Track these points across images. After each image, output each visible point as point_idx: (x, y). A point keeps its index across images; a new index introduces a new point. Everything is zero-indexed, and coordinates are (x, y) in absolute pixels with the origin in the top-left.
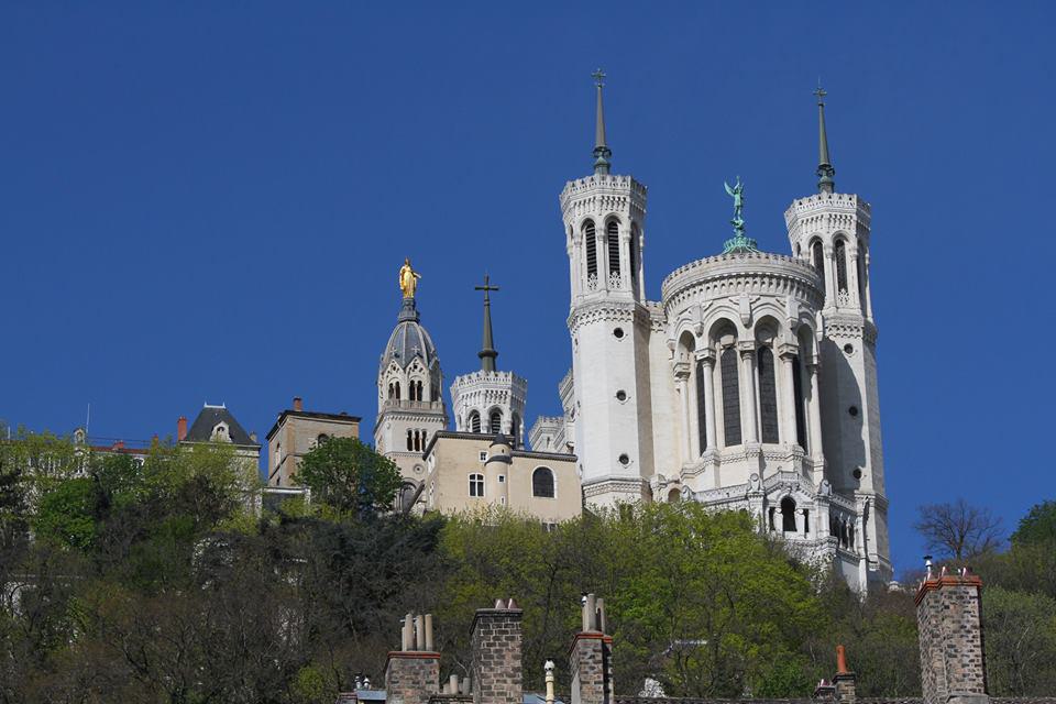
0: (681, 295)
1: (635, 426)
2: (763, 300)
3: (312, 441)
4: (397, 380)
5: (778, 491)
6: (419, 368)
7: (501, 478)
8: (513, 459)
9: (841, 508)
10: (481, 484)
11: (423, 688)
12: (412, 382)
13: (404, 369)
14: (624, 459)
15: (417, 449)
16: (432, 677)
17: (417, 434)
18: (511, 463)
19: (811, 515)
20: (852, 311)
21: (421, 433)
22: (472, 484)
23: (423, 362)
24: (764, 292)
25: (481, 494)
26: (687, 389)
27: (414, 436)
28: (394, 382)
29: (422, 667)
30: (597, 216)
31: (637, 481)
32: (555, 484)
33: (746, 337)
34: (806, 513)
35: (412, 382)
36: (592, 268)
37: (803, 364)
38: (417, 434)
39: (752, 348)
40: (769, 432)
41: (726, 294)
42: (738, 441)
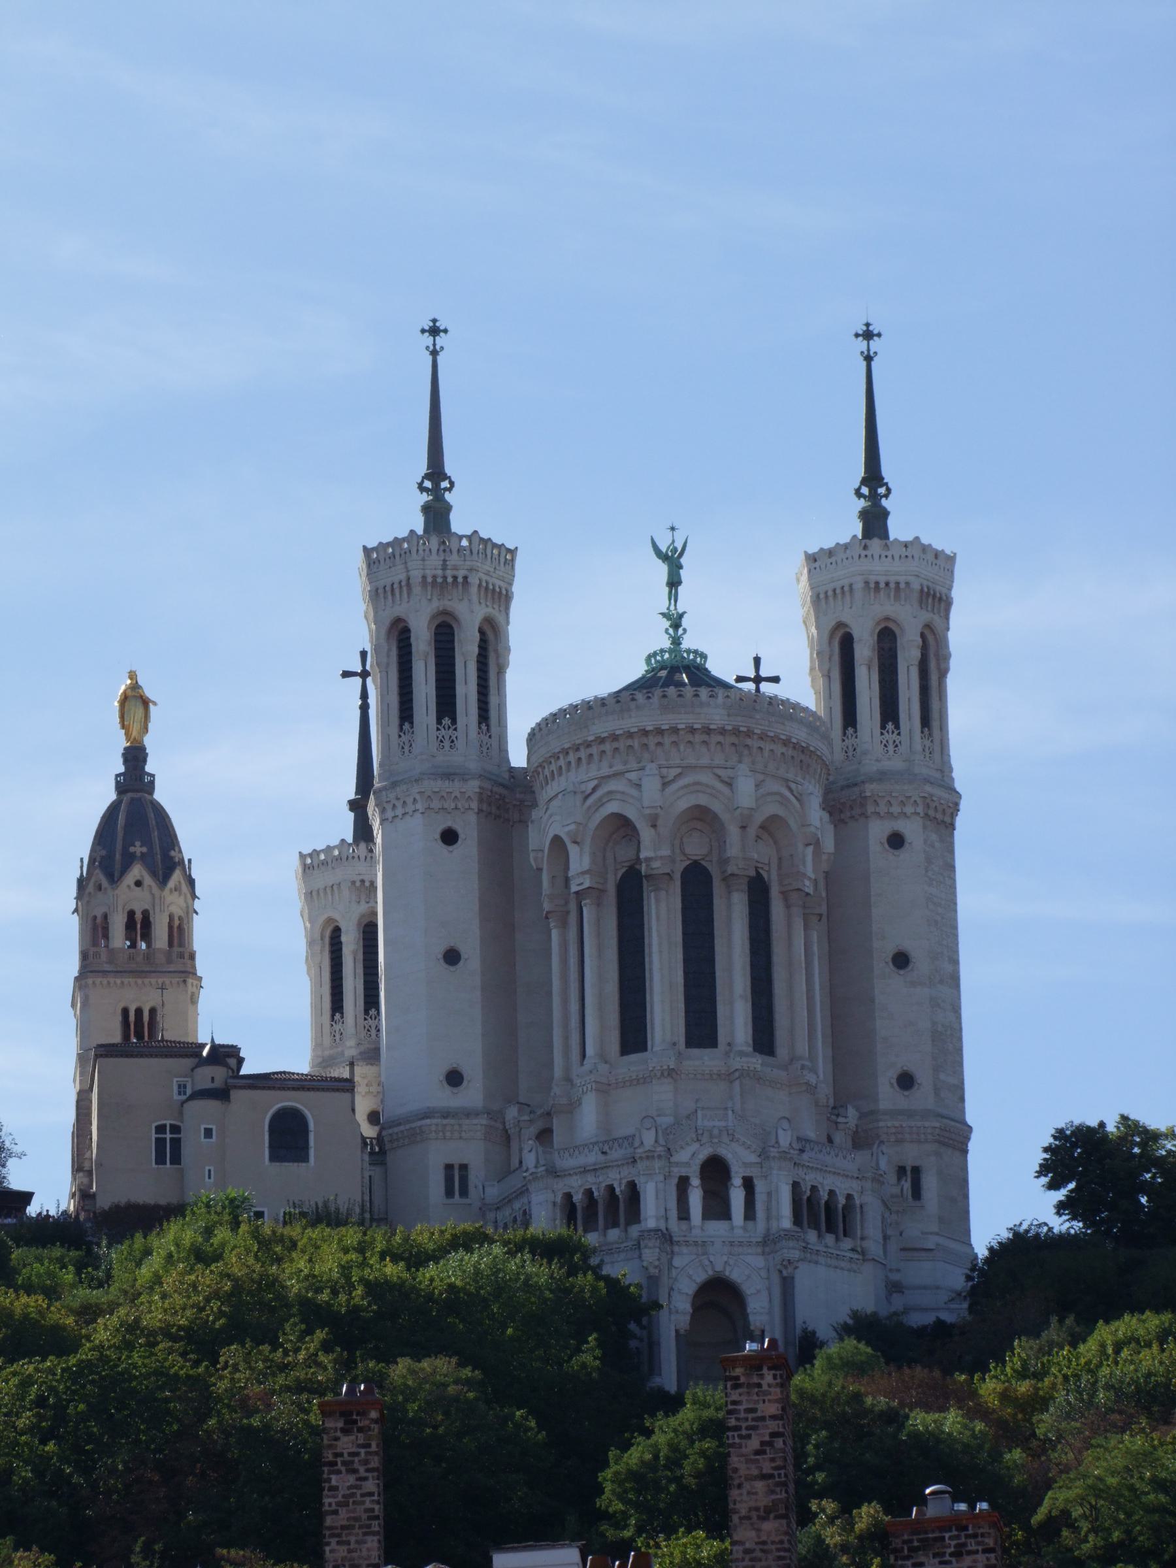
7: (208, 1133)
10: (176, 1143)
12: (131, 914)
14: (454, 1078)
17: (139, 1012)
19: (760, 1187)
22: (160, 1143)
24: (691, 761)
25: (176, 1159)
34: (748, 1184)
38: (139, 1012)
41: (619, 767)
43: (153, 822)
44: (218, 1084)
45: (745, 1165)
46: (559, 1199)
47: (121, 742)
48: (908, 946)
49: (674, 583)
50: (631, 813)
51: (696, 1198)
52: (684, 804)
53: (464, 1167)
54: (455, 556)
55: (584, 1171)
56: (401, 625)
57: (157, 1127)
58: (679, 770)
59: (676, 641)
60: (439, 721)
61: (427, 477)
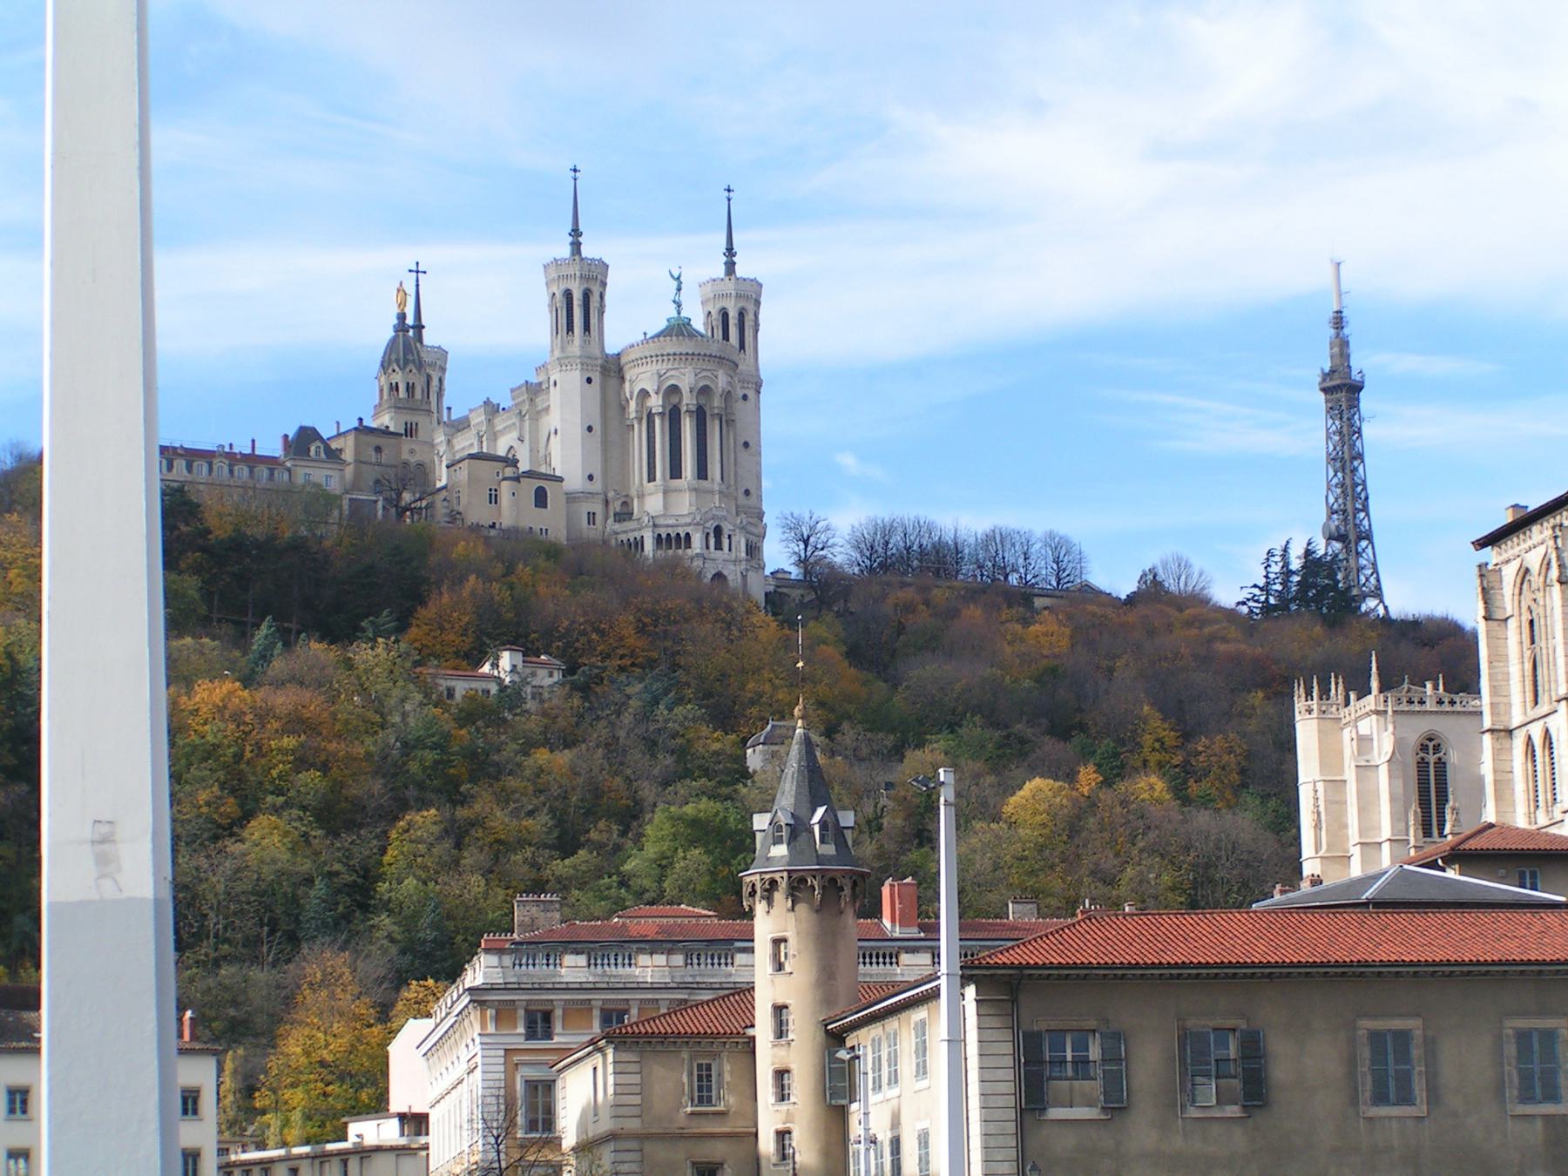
0: (639, 362)
1: (599, 452)
2: (704, 374)
10: (496, 495)
14: (591, 478)
18: (519, 482)
19: (733, 539)
22: (491, 495)
27: (409, 425)
32: (549, 499)
33: (688, 401)
34: (729, 537)
37: (724, 420)
40: (702, 472)
41: (676, 366)
45: (730, 530)
46: (656, 535)
47: (395, 310)
48: (748, 440)
49: (679, 289)
51: (712, 541)
52: (701, 384)
53: (594, 514)
55: (668, 526)
59: (679, 313)
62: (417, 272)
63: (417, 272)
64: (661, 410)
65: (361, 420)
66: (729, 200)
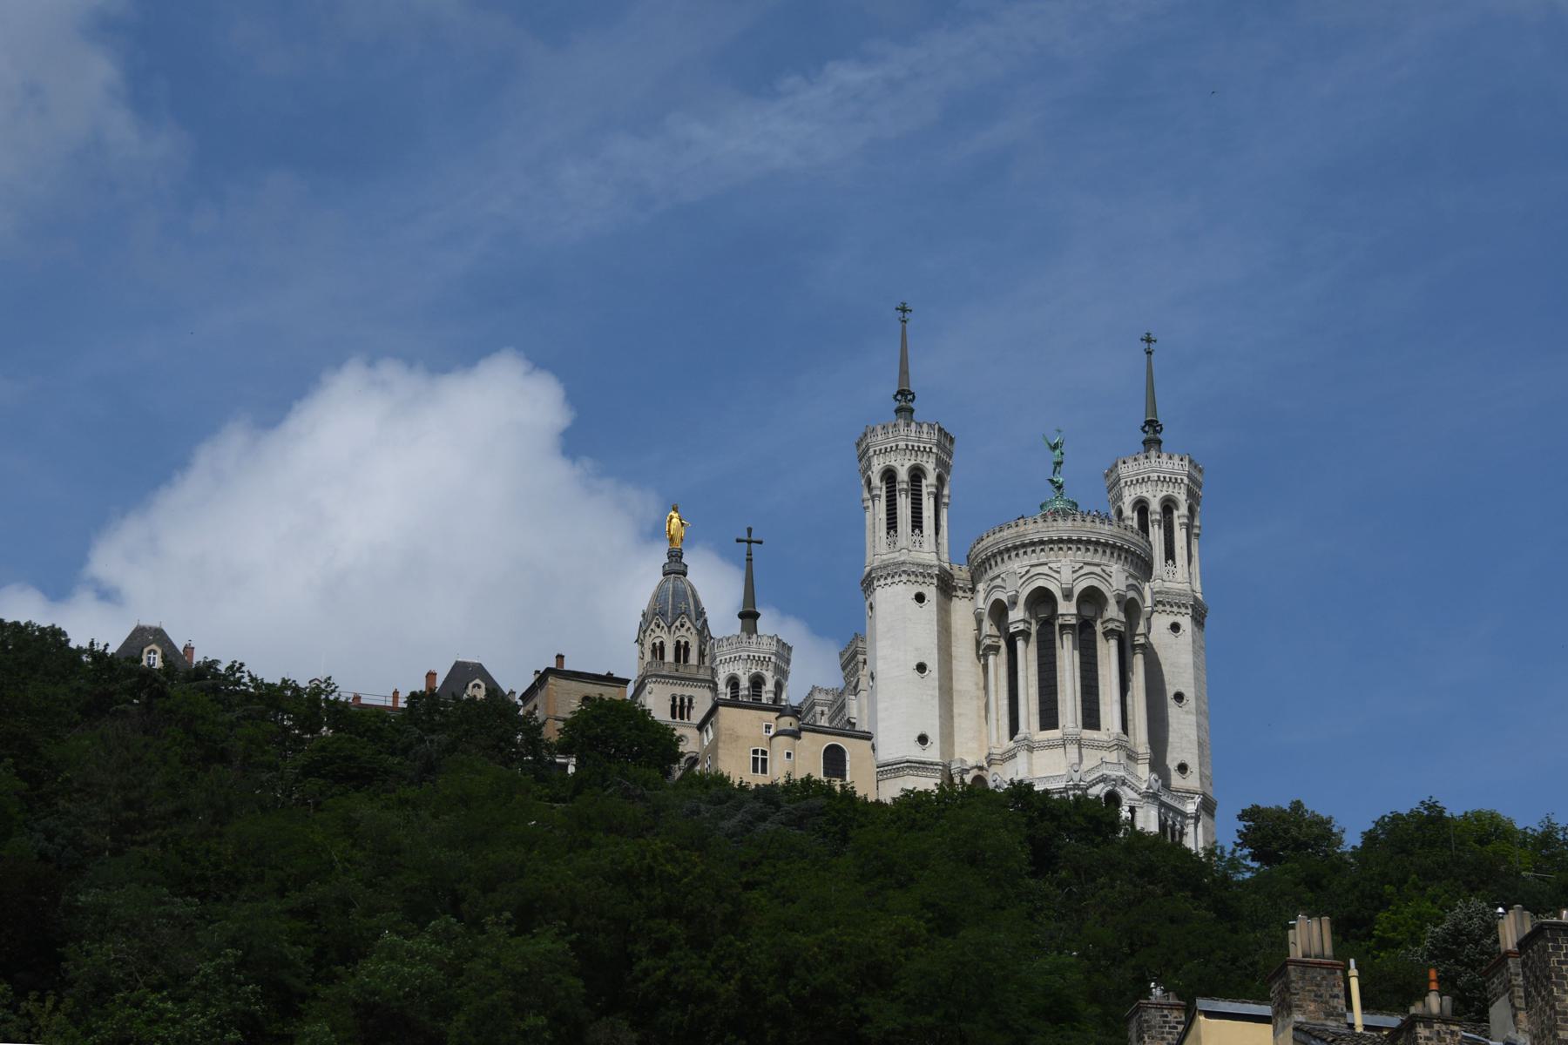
1: (936, 702)
2: (1087, 569)
3: (575, 704)
4: (661, 639)
5: (1102, 785)
6: (686, 627)
7: (789, 755)
8: (803, 734)
9: (1169, 808)
10: (764, 761)
11: (1327, 1003)
12: (678, 642)
13: (669, 628)
14: (923, 739)
15: (682, 717)
16: (1336, 991)
17: (682, 700)
18: (800, 738)
20: (1180, 586)
21: (686, 700)
22: (756, 760)
23: (691, 621)
24: (1088, 560)
26: (996, 665)
27: (678, 700)
28: (657, 641)
29: (1324, 978)
30: (899, 467)
31: (937, 764)
35: (678, 642)
36: (892, 524)
37: (1128, 644)
38: (682, 700)
39: (1074, 621)
40: (1091, 718)
42: (1054, 726)
43: (689, 592)
44: (794, 727)
50: (1054, 588)
54: (925, 436)
56: (889, 474)
57: (754, 751)
58: (1082, 564)
60: (913, 531)
61: (898, 393)
62: (750, 542)
63: (750, 542)
64: (1022, 626)
65: (560, 657)
66: (1149, 353)
